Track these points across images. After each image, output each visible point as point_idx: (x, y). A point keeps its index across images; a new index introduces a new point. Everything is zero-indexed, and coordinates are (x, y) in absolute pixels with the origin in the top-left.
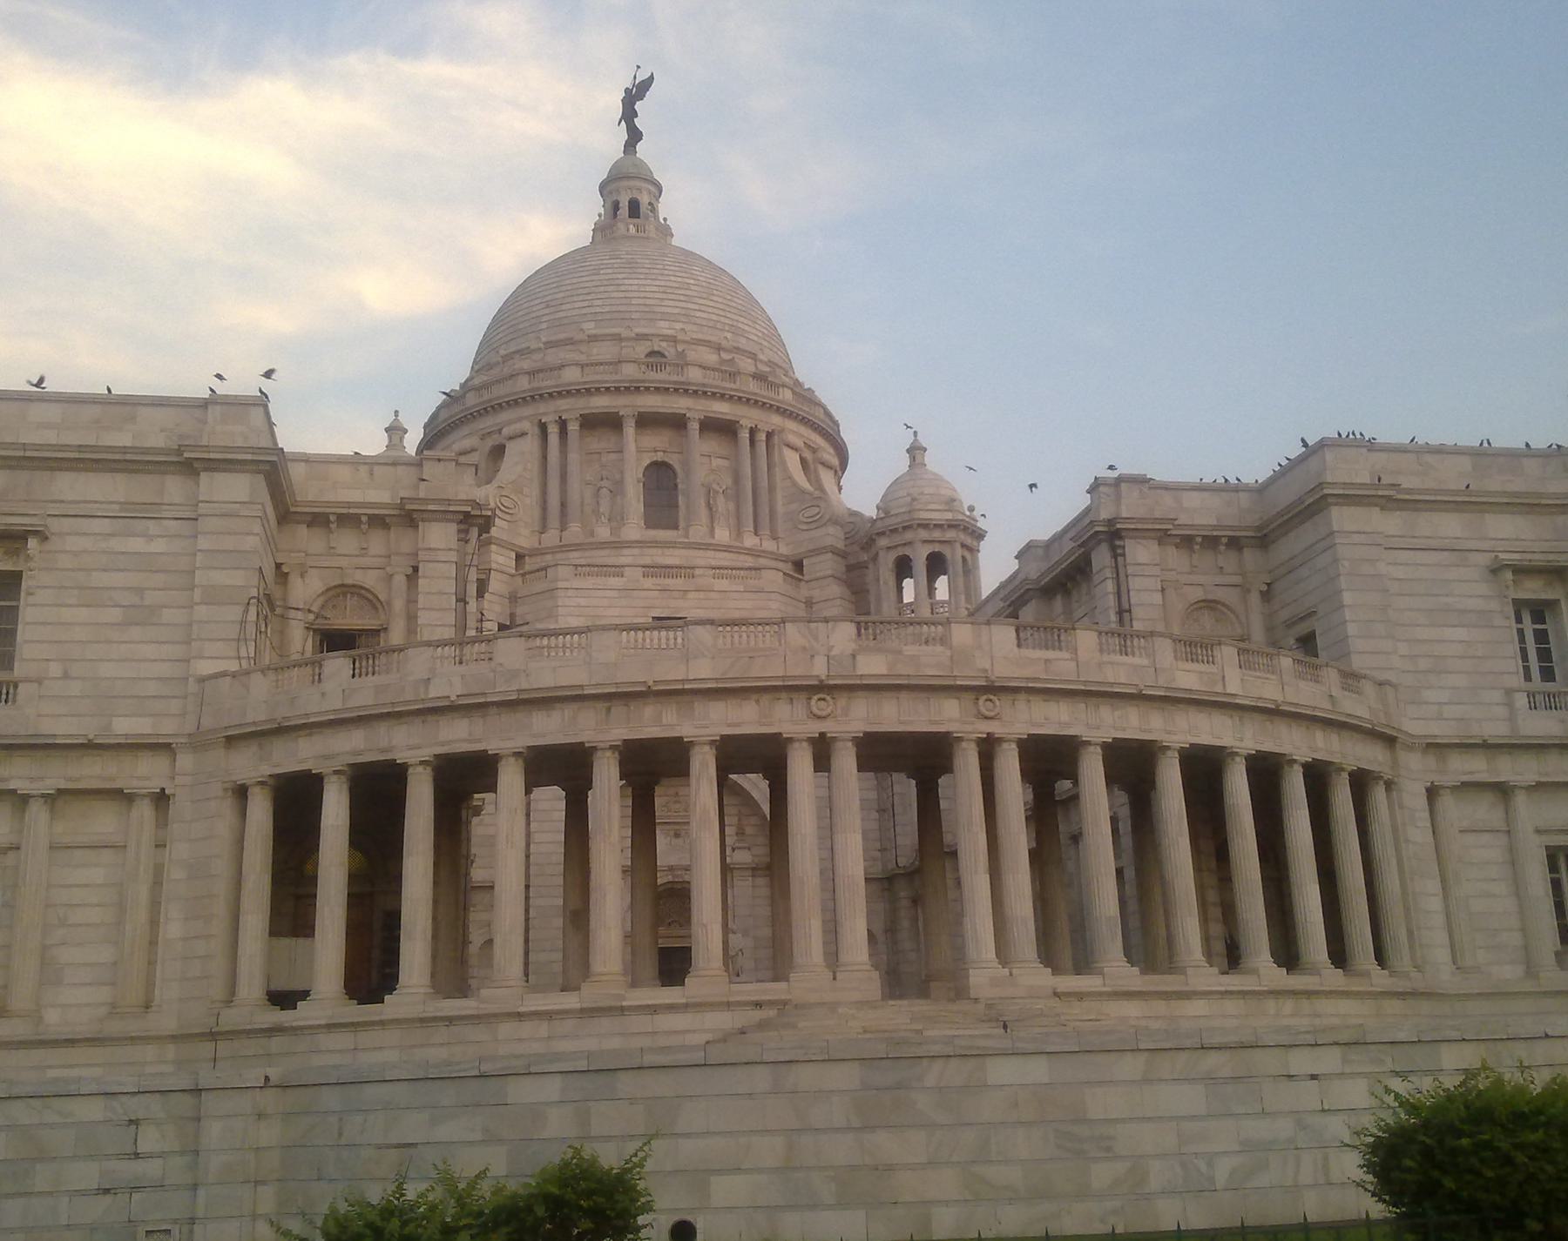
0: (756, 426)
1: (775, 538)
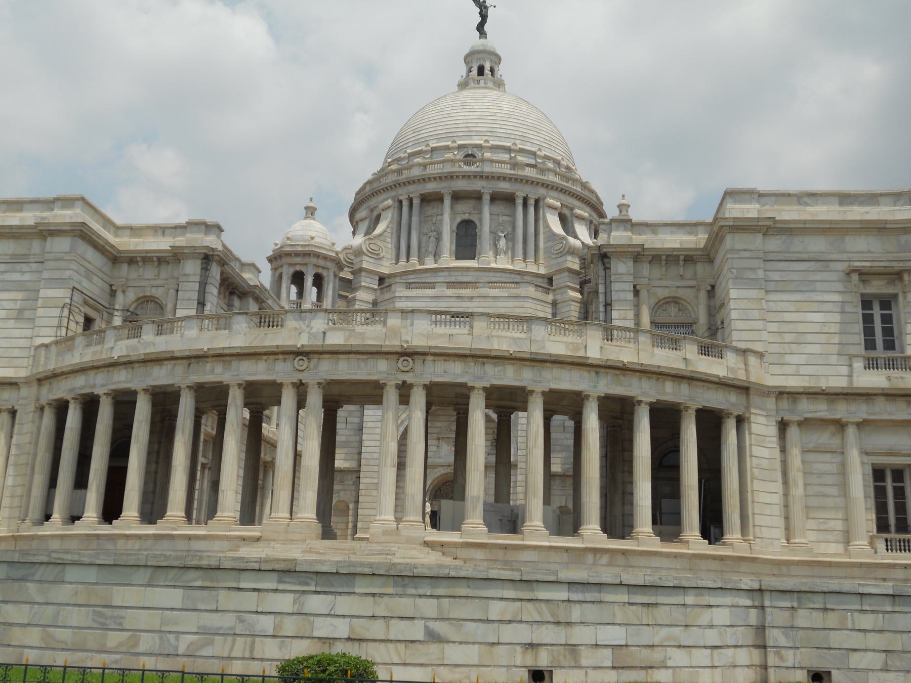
0: (527, 195)
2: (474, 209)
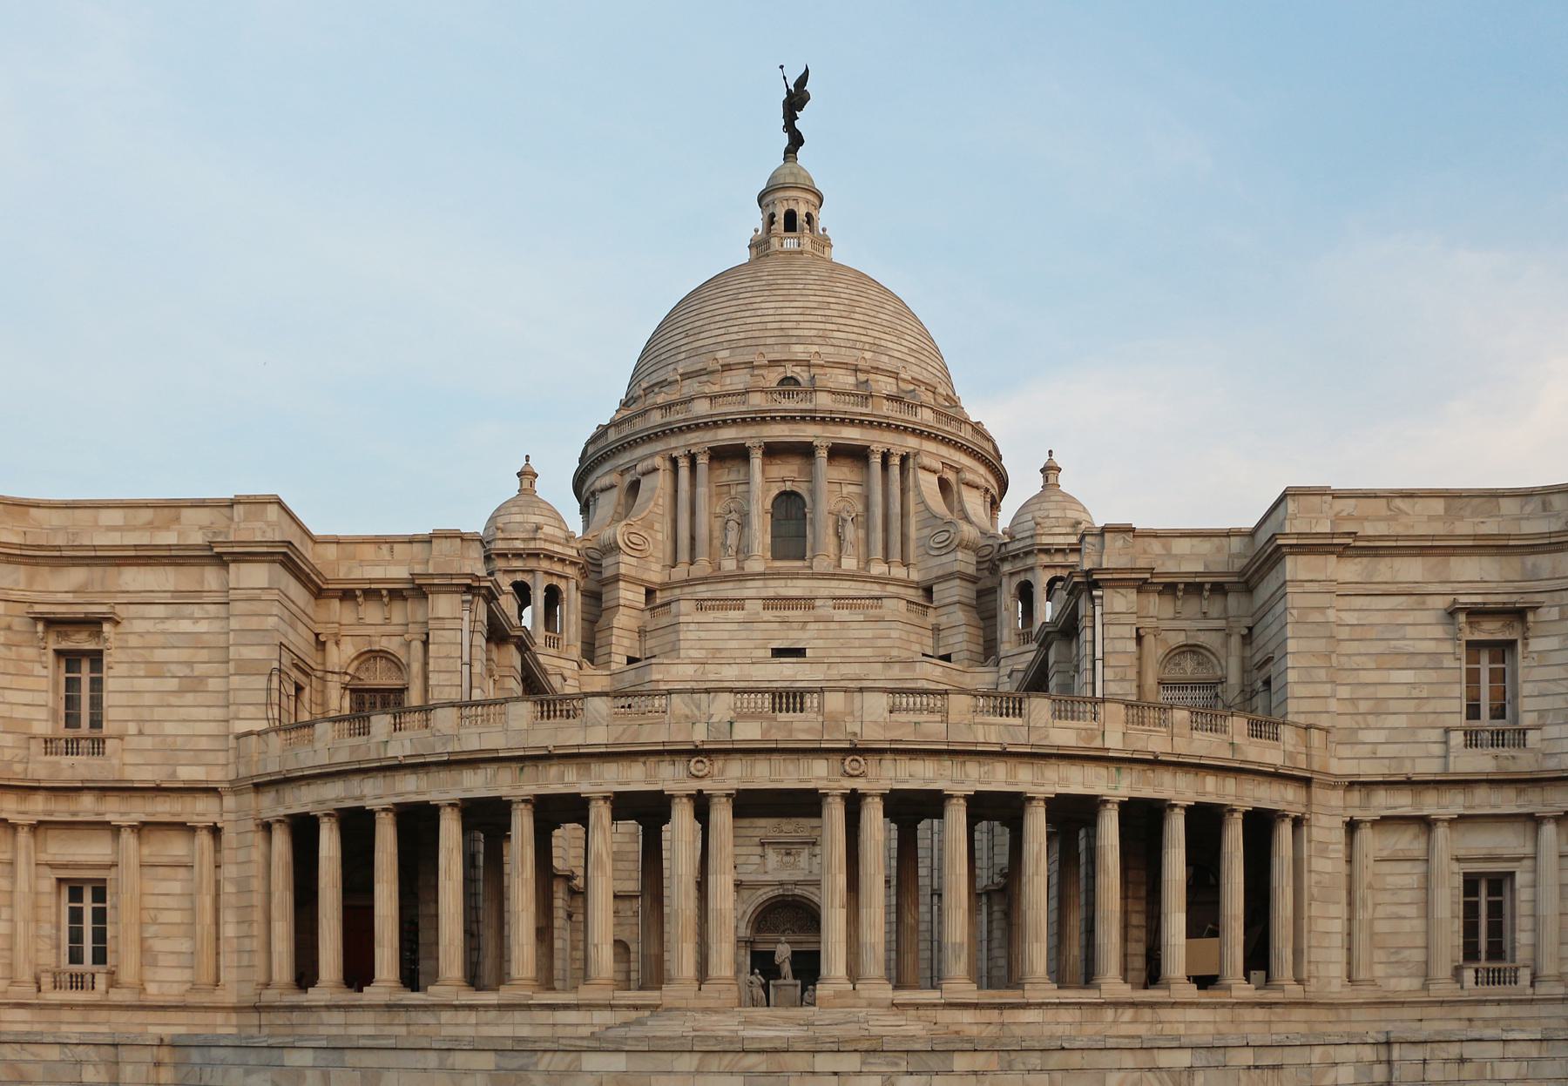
0: (888, 450)
1: (905, 563)
2: (800, 473)
